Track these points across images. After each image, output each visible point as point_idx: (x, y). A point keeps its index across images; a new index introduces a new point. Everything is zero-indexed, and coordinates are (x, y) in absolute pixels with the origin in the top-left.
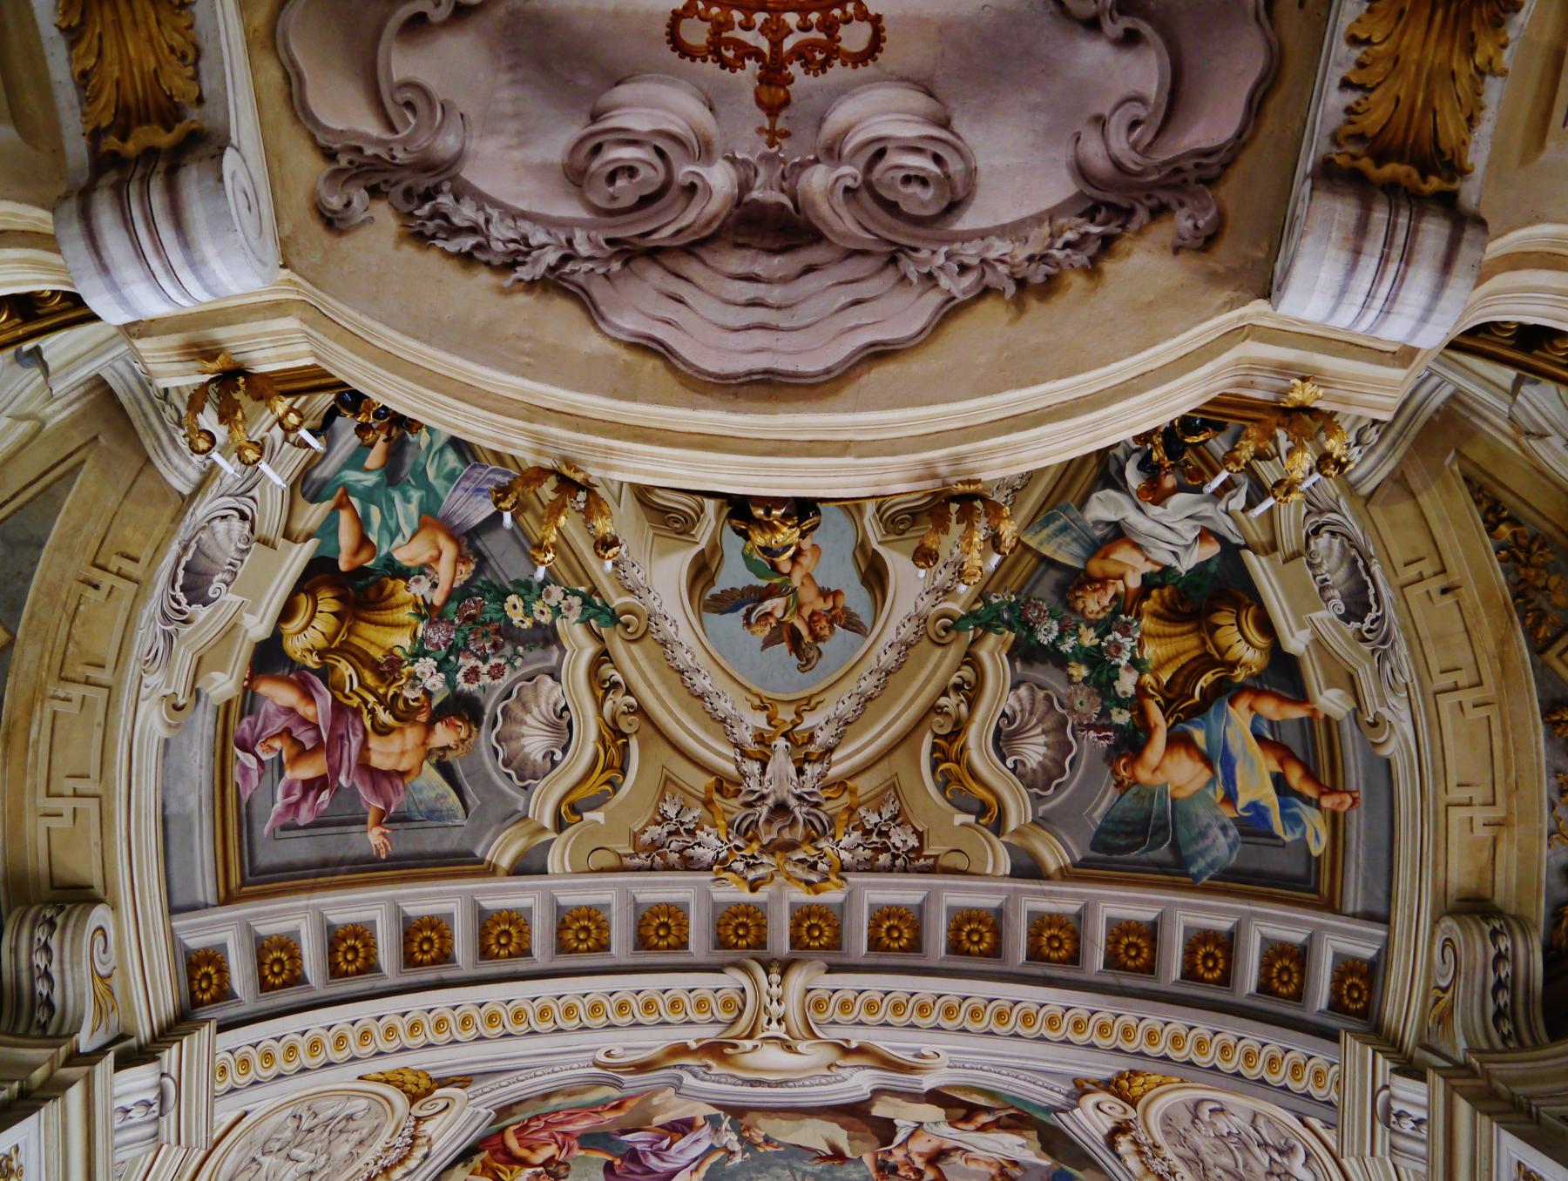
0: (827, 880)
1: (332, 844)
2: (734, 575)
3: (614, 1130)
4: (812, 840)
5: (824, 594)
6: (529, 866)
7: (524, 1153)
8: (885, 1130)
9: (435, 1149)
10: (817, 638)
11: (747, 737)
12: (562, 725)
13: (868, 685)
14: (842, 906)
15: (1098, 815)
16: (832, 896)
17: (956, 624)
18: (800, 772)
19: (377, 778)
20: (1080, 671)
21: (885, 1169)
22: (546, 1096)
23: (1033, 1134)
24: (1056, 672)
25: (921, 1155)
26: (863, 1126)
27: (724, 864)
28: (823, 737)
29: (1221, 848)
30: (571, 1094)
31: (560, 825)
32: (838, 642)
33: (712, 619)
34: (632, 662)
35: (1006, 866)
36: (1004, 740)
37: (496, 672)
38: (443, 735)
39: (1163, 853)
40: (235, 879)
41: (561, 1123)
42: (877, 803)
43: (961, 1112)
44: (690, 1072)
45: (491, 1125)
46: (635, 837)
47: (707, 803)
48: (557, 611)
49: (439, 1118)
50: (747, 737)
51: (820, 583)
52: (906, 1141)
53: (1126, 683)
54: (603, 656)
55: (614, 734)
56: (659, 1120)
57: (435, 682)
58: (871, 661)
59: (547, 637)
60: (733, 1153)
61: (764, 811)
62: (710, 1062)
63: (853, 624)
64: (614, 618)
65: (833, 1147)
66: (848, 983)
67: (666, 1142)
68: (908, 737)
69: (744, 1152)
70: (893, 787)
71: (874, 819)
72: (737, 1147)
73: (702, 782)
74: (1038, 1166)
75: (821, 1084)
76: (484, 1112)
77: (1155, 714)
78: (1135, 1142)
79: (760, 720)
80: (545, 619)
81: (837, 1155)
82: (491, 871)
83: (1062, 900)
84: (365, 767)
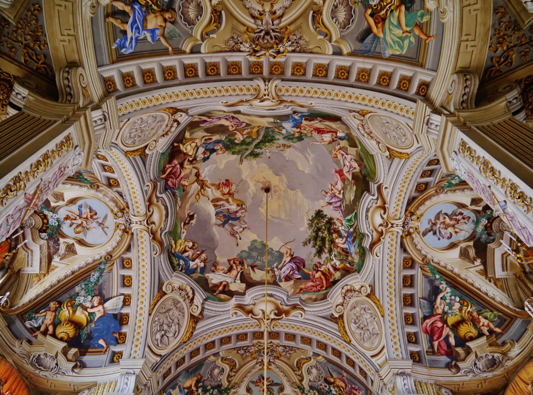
0: (257, 344)
1: (353, 380)
2: (276, 389)
3: (302, 280)
4: (259, 350)
5: (258, 386)
6: (316, 355)
7: (323, 277)
8: (243, 279)
9: (340, 290)
10: (259, 379)
11: (273, 365)
12: (309, 372)
13: (249, 375)
14: (253, 340)
15: (203, 368)
16: (255, 341)
17: (233, 387)
18: (262, 360)
19: (344, 382)
20: (209, 387)
21: (242, 263)
22: (316, 300)
23: (210, 285)
24: (212, 385)
25: (234, 269)
26: (247, 279)
27: (277, 346)
28: (258, 365)
29: (180, 379)
30: (310, 299)
31: (310, 358)
32: (255, 379)
33: (280, 382)
34: (296, 379)
35: (221, 354)
36: (223, 370)
37: (321, 385)
38: (332, 380)
39: (190, 370)
40: (369, 392)
41: (313, 286)
42: (247, 356)
43: (226, 289)
44: (285, 302)
45: (328, 293)
46: (295, 352)
47: (281, 355)
48: (309, 392)
49: (338, 303)
50: (273, 365)
51: (259, 388)
52: (238, 274)
53: (200, 390)
54: (301, 381)
55: (299, 367)
56: (292, 282)
57: (332, 389)
58: (248, 378)
59: (311, 388)
60: (276, 267)
61: (269, 354)
62: (280, 306)
63: (253, 382)
64: (299, 387)
65: (254, 270)
66: (252, 329)
67: (291, 273)
68: (241, 367)
69: (274, 268)
70: (243, 359)
71: (247, 354)
72: (275, 269)
73: (282, 358)
74: (208, 273)
75: (257, 296)
76: (329, 299)
77: (194, 388)
78: (189, 297)
79: (270, 367)
80: (311, 391)
81: (253, 267)
82: (323, 357)
83: (208, 353)
84: (346, 385)
